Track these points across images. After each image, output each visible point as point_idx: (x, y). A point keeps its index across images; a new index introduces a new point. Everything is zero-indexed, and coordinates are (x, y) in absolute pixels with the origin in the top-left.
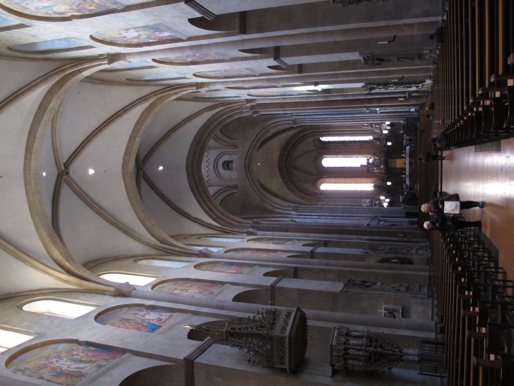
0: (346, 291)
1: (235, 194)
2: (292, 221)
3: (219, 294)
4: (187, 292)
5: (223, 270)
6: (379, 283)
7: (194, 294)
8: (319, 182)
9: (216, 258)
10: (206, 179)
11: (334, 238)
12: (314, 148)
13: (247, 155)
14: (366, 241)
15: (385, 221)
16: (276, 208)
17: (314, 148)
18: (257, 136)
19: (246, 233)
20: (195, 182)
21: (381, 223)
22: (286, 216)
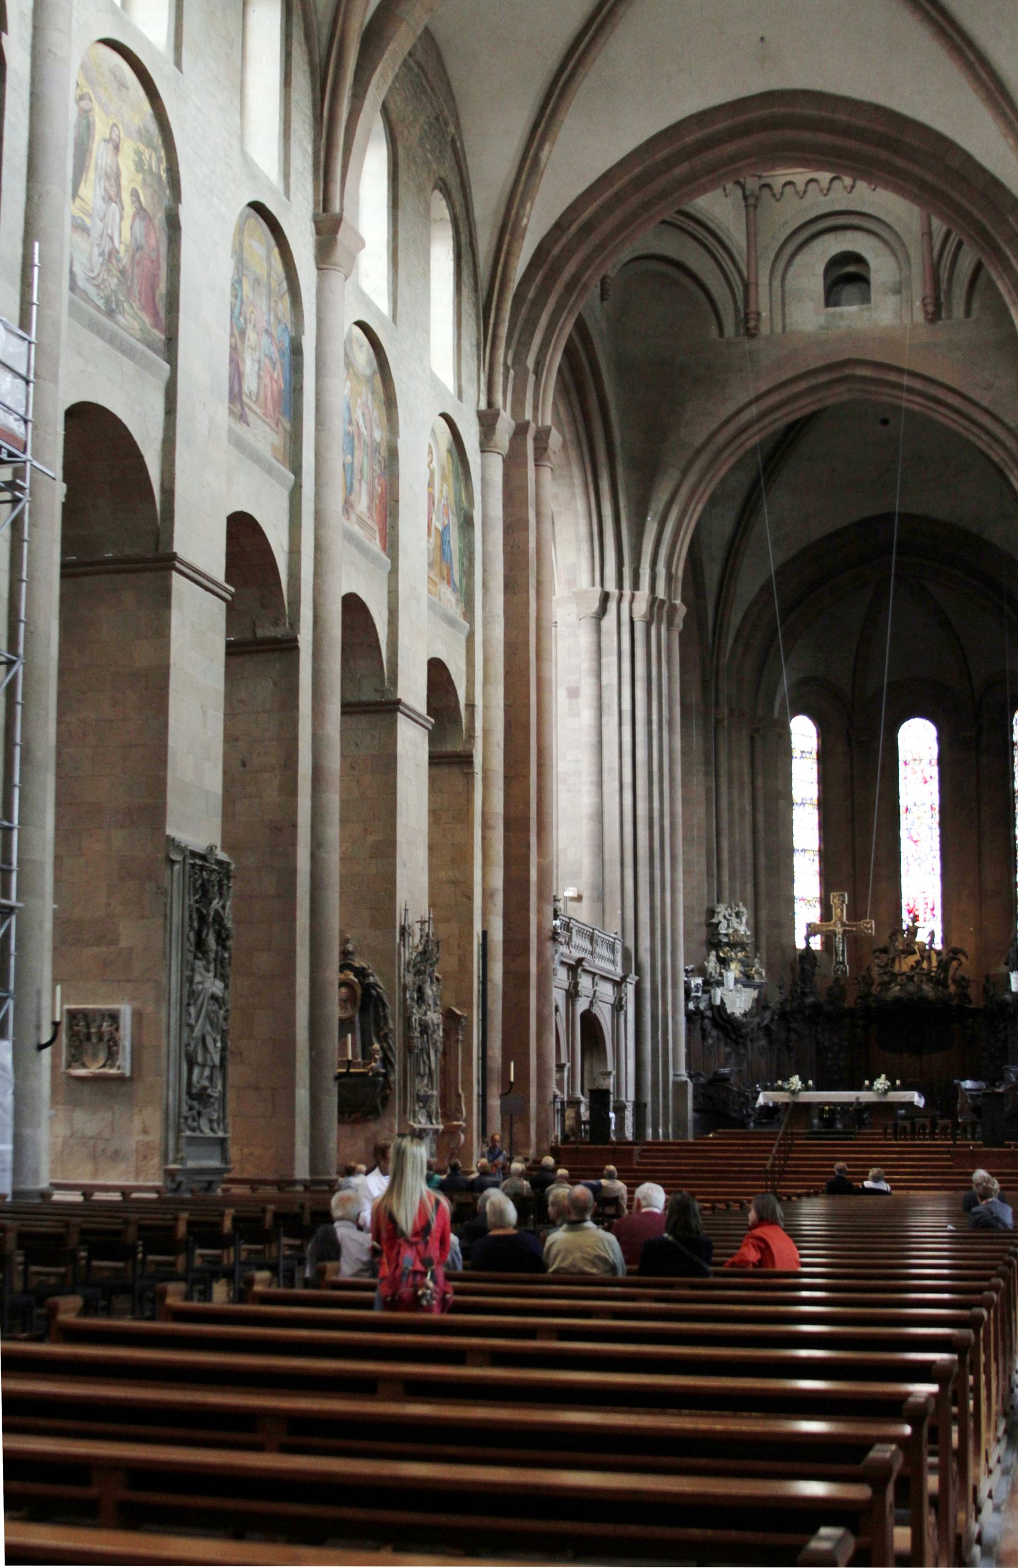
0: (173, 862)
1: (714, 329)
2: (605, 597)
3: (112, 340)
4: (109, 199)
5: (251, 336)
6: (217, 987)
7: (95, 234)
9: (320, 291)
10: (779, 176)
11: (488, 797)
14: (478, 928)
15: (618, 1007)
19: (490, 404)
20: (709, 143)
21: (606, 990)
22: (627, 571)
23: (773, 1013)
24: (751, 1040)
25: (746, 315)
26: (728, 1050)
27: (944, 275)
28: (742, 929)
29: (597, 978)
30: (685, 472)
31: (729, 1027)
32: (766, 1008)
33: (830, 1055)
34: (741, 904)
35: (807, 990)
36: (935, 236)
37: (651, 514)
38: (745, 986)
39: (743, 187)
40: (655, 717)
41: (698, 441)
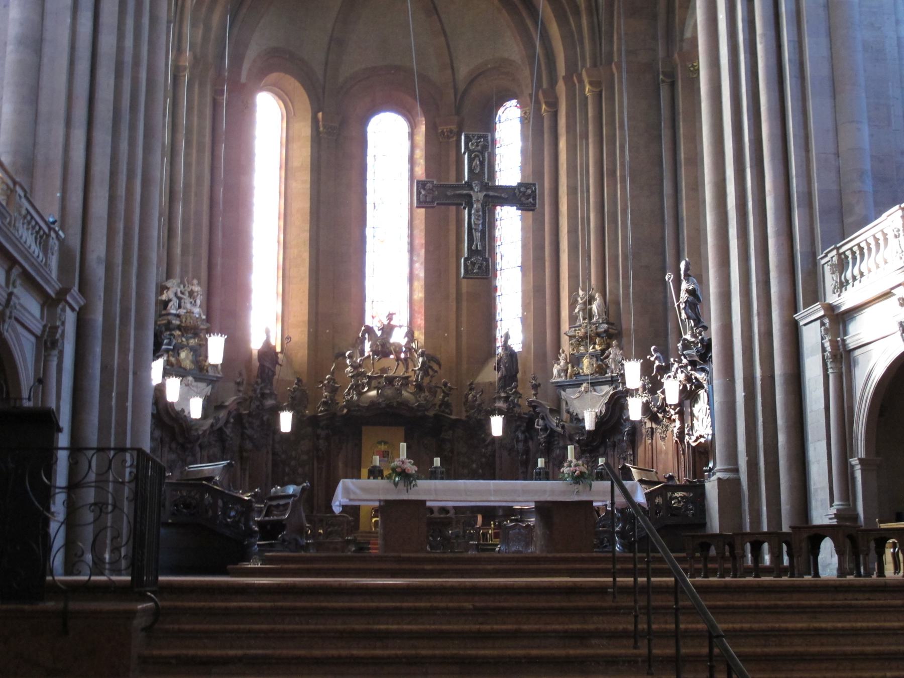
8: (293, 84)
12: (463, 71)
15: (48, 342)
17: (463, 71)
23: (229, 413)
24: (200, 446)
26: (173, 456)
28: (197, 310)
29: (16, 271)
31: (177, 429)
32: (220, 407)
33: (287, 470)
34: (195, 282)
35: (268, 391)
38: (197, 379)
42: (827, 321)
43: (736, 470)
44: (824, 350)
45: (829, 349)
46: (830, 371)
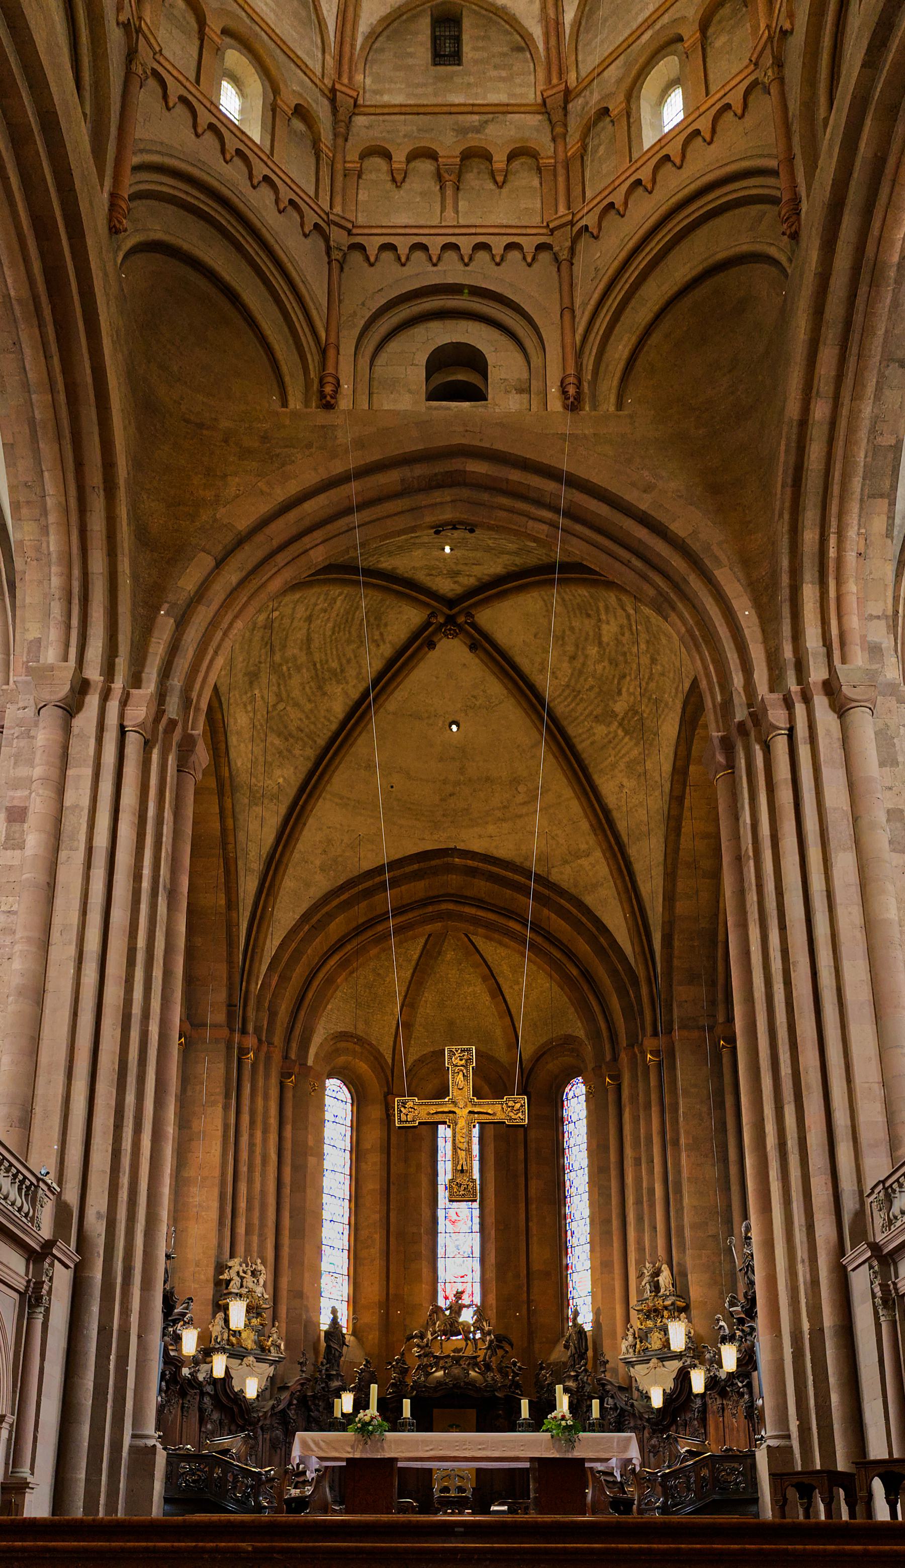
13: (525, 465)
16: (182, 623)
18: (644, 520)
25: (322, 384)
27: (589, 363)
30: (220, 563)
36: (578, 313)
37: (166, 606)
39: (327, 239)
40: (146, 872)
41: (242, 525)
42: (875, 1263)
43: (788, 1437)
44: (874, 1296)
45: (879, 1294)
46: (882, 1319)
